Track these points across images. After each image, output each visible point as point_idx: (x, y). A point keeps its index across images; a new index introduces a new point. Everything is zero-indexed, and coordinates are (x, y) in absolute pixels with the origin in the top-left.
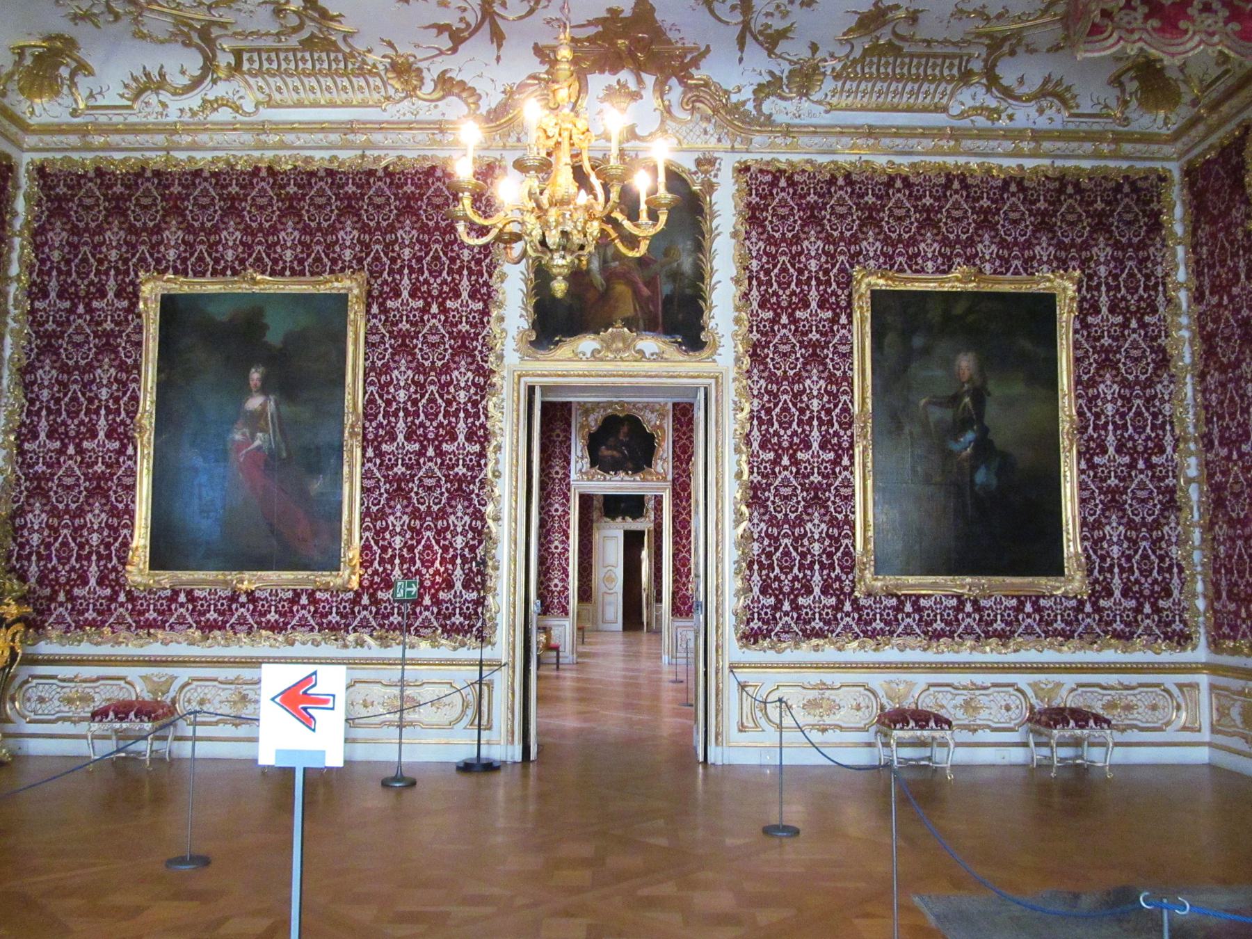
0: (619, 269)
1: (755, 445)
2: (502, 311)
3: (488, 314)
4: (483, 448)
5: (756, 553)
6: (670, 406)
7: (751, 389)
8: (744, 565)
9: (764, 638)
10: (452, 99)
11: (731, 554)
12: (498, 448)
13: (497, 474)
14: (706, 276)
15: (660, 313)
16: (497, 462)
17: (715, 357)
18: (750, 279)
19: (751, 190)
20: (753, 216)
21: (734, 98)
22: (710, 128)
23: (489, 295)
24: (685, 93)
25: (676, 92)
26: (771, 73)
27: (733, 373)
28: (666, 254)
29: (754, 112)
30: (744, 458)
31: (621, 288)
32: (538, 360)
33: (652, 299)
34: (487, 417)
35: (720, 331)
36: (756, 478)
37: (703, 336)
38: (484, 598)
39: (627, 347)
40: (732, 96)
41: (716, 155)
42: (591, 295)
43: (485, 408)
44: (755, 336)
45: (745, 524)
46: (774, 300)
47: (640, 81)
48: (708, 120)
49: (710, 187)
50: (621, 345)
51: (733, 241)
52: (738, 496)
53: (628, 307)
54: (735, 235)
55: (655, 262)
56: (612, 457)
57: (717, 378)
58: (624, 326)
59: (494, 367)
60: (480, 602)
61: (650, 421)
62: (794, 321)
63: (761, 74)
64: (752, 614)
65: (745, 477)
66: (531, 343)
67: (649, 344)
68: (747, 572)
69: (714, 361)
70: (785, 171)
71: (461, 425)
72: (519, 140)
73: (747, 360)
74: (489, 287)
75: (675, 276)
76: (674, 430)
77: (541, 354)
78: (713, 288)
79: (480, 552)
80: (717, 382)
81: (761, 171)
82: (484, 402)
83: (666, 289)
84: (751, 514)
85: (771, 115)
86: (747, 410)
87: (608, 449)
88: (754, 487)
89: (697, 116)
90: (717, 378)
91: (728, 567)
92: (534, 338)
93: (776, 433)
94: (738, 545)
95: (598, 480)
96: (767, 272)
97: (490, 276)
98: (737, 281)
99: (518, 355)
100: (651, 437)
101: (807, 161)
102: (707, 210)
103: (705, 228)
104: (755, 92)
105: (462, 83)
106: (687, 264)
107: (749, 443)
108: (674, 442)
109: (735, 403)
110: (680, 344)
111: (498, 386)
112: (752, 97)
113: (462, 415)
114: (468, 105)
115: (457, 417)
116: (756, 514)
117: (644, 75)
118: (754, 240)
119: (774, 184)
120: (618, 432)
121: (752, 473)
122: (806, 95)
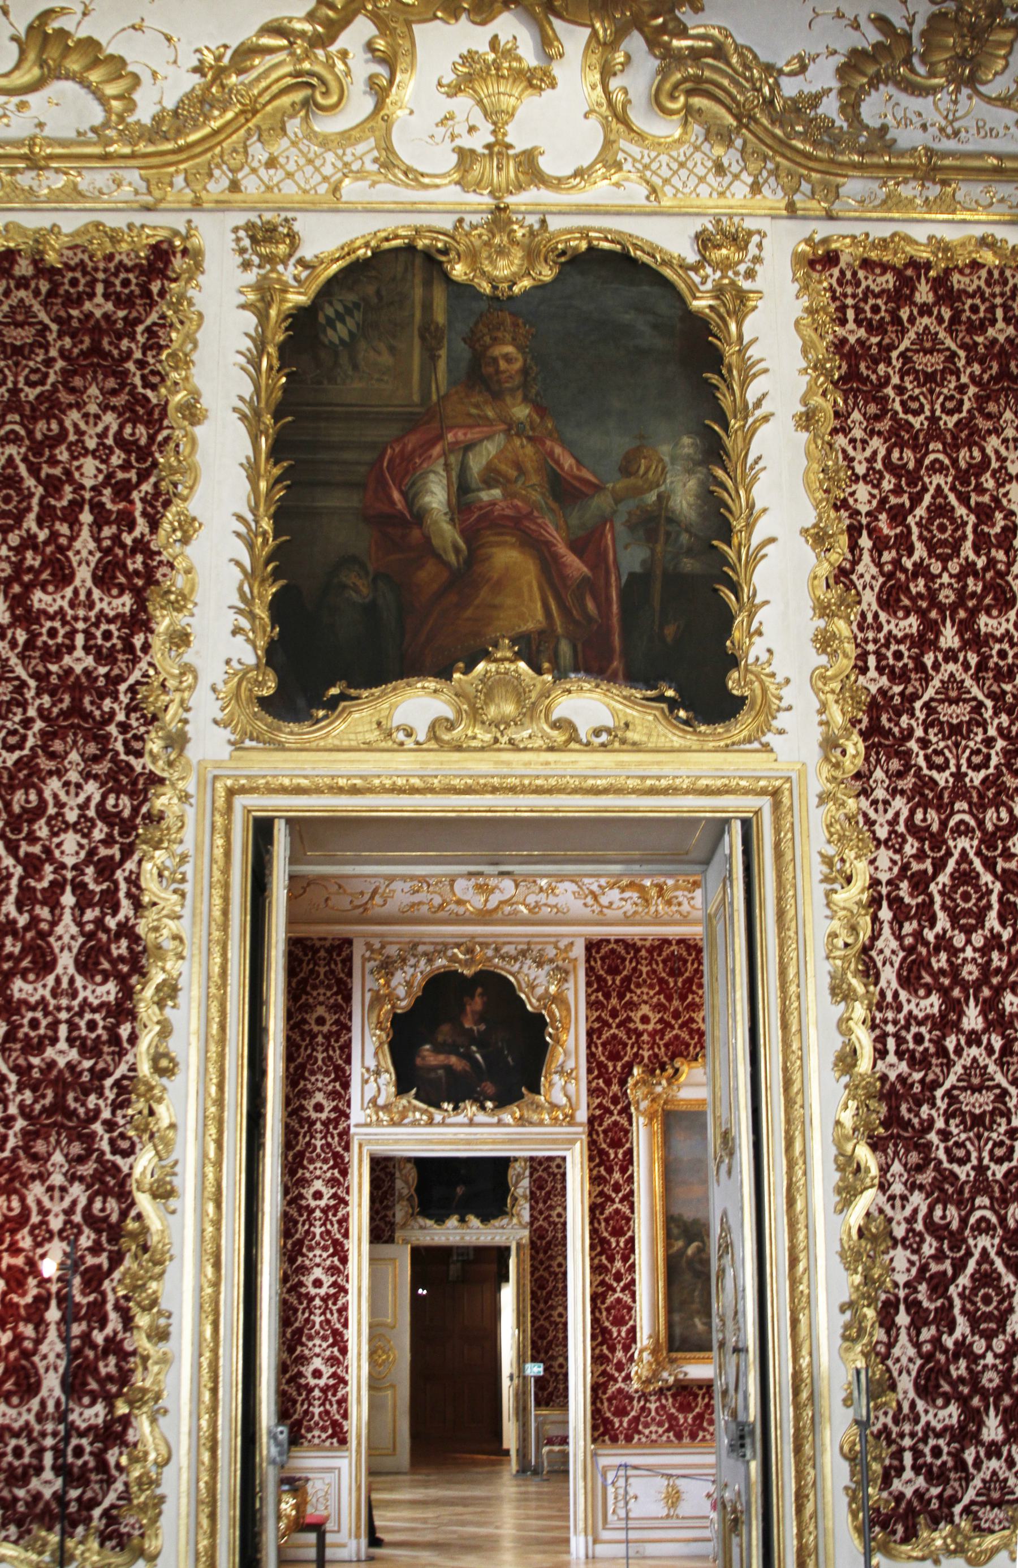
0: (503, 508)
1: (889, 975)
2: (182, 620)
3: (147, 626)
4: (127, 992)
5: (901, 1279)
6: (579, 951)
7: (870, 823)
8: (870, 1313)
9: (935, 1521)
10: (64, 88)
11: (831, 1285)
12: (169, 992)
13: (165, 1066)
14: (738, 525)
15: (615, 620)
16: (166, 1030)
17: (769, 738)
18: (854, 532)
19: (842, 309)
20: (853, 375)
21: (790, 87)
22: (731, 158)
23: (149, 576)
24: (664, 73)
25: (639, 72)
26: (882, 22)
27: (817, 783)
28: (627, 469)
29: (840, 122)
30: (860, 1011)
31: (507, 557)
32: (281, 747)
33: (591, 586)
34: (138, 905)
35: (781, 667)
36: (896, 1068)
37: (734, 682)
38: (126, 1421)
39: (529, 712)
40: (784, 81)
41: (749, 224)
42: (428, 575)
43: (133, 881)
44: (874, 682)
45: (868, 1199)
46: (919, 586)
47: (546, 42)
48: (725, 137)
49: (738, 302)
50: (509, 708)
51: (804, 436)
52: (847, 1118)
53: (529, 608)
54: (807, 419)
55: (598, 488)
56: (448, 1068)
57: (775, 793)
58: (519, 656)
59: (159, 769)
60: (114, 1433)
61: (533, 985)
62: (975, 641)
63: (856, 26)
64: (898, 1454)
65: (864, 1065)
66: (264, 702)
67: (588, 704)
68: (880, 1334)
69: (767, 748)
70: (928, 266)
71: (67, 927)
72: (235, 186)
73: (855, 745)
74: (150, 554)
75: (653, 524)
76: (591, 1005)
77: (289, 733)
78: (755, 558)
79: (113, 1288)
80: (777, 805)
81: (866, 264)
82: (130, 865)
83: (630, 557)
84: (884, 1170)
85: (884, 129)
86: (861, 880)
87: (437, 1049)
88: (891, 1093)
89: (697, 130)
90: (775, 793)
91: (826, 1322)
92: (269, 687)
93: (943, 943)
94: (850, 1258)
95: (415, 1123)
96: (898, 515)
97: (154, 525)
98: (819, 538)
99: (226, 734)
100: (537, 1023)
101: (983, 242)
102: (730, 352)
103: (726, 402)
104: (842, 72)
105: (91, 44)
106: (683, 495)
107: (870, 972)
108: (590, 1033)
109: (828, 861)
110: (673, 705)
111: (170, 820)
112: (835, 84)
113: (68, 899)
114: (103, 100)
115: (55, 905)
116: (897, 1167)
117: (557, 23)
118: (858, 433)
119: (902, 294)
120: (462, 1010)
121: (881, 1053)
122: (972, 81)
